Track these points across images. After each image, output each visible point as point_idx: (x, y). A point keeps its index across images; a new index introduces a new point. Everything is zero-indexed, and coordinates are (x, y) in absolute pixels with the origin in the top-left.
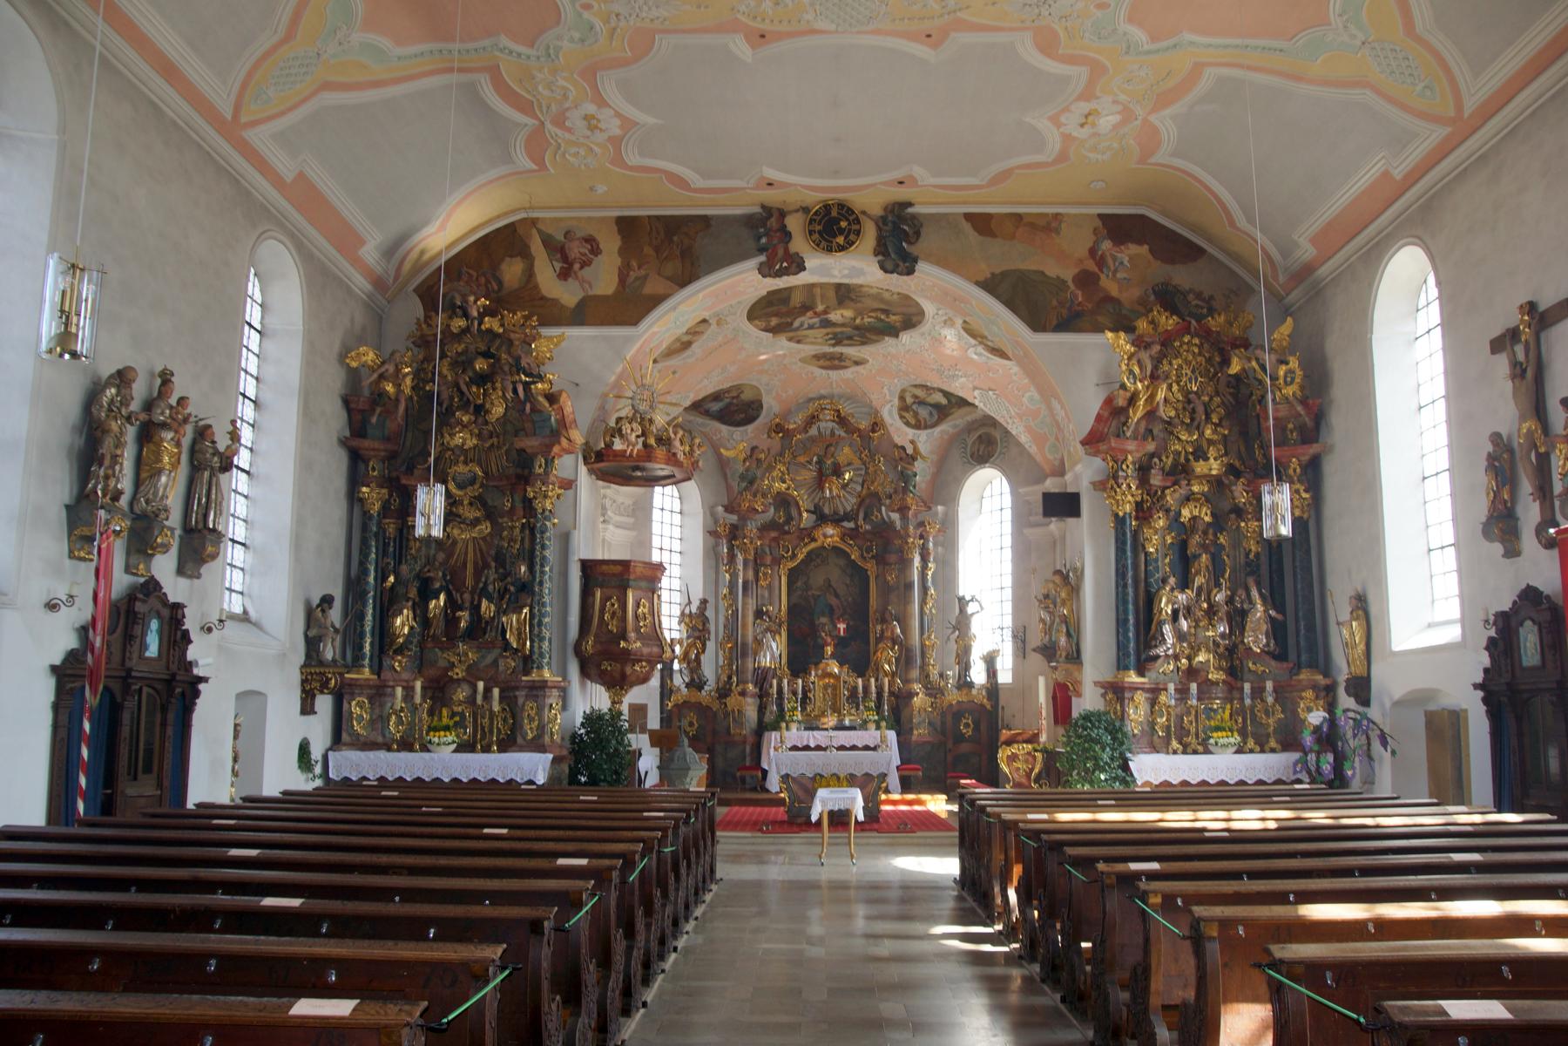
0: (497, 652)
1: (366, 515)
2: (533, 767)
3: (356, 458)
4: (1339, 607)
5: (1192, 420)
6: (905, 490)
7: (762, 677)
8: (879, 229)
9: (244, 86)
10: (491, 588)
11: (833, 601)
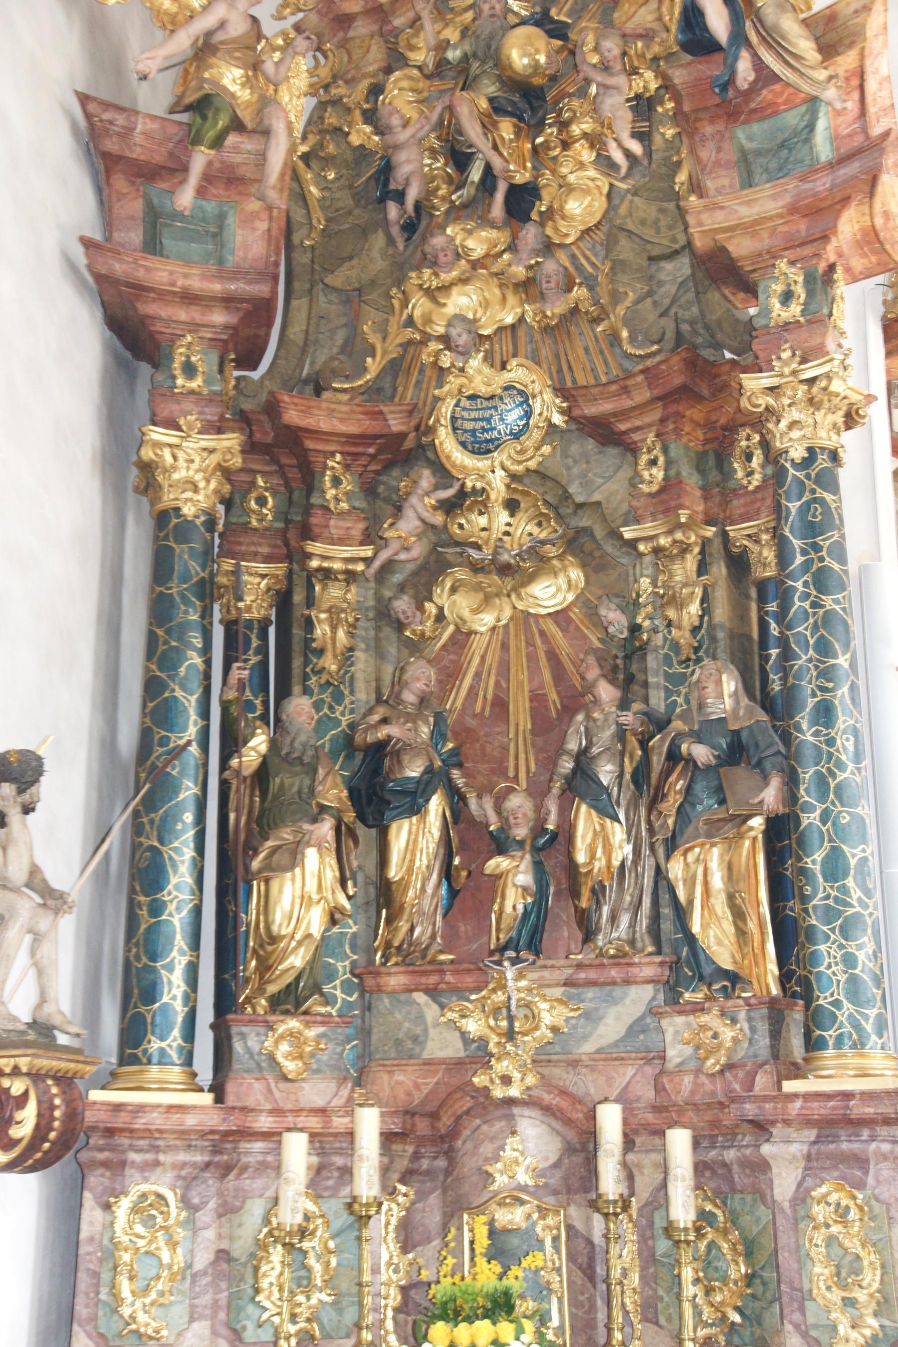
0: (639, 998)
3: (133, 337)
10: (606, 773)
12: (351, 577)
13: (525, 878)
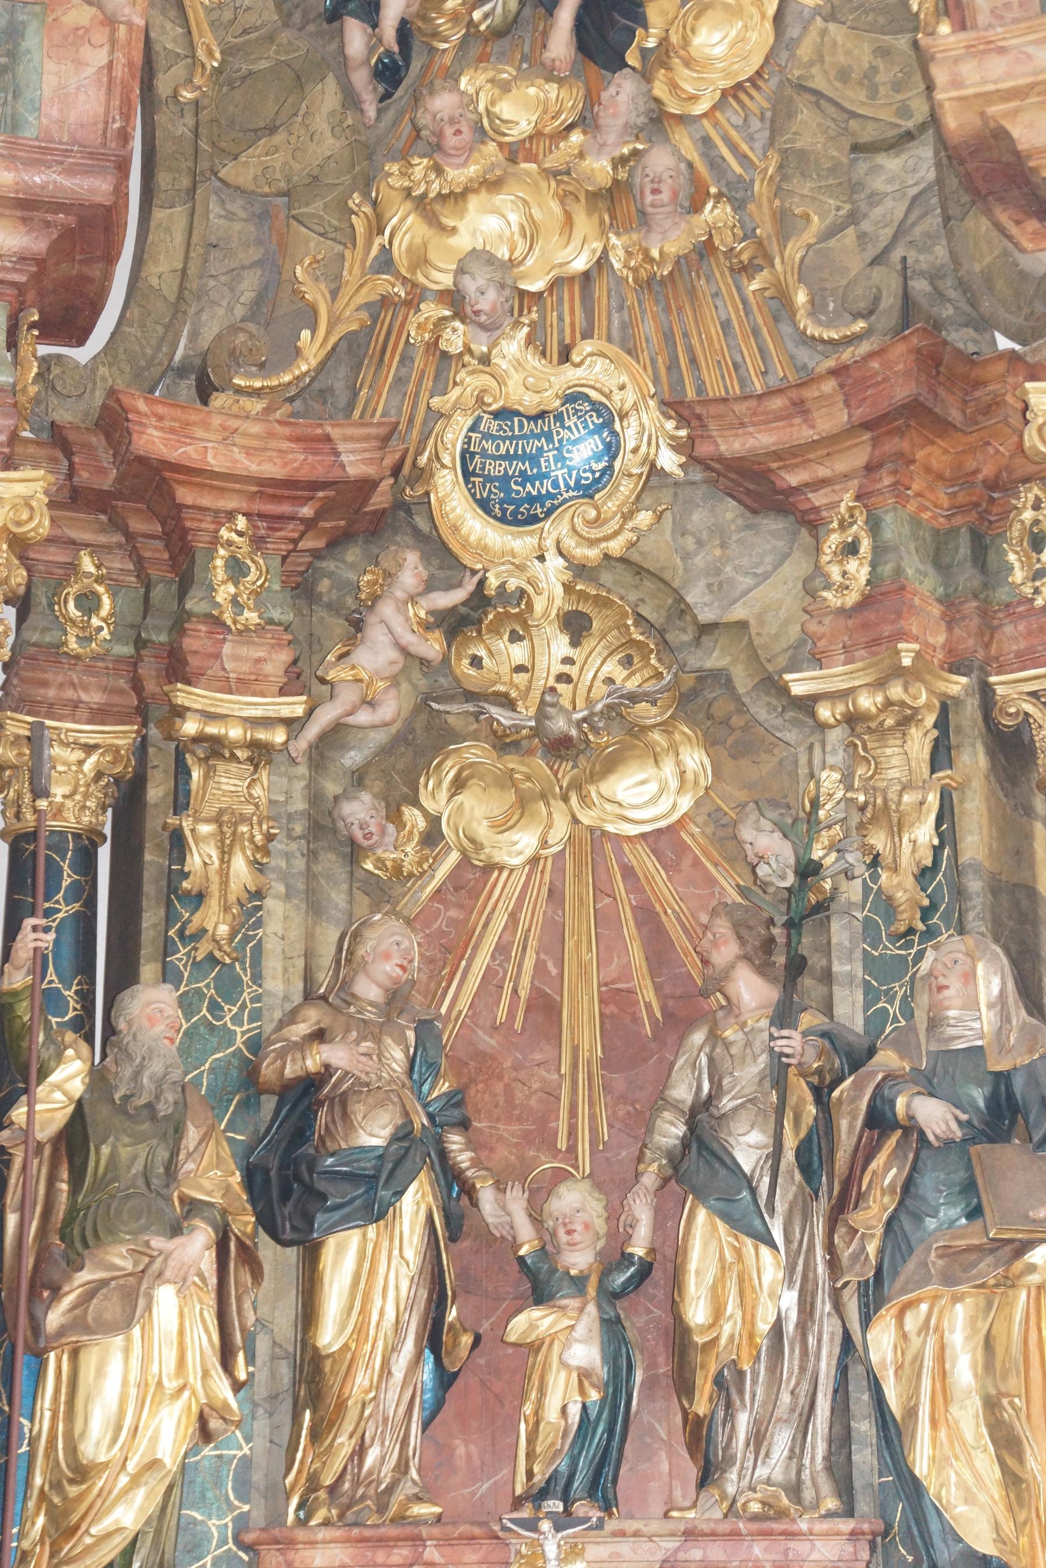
10: (748, 1147)
12: (260, 754)
13: (585, 1351)
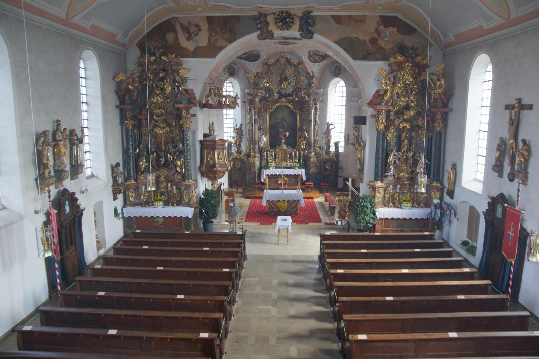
1: (127, 130)
2: (188, 212)
4: (448, 167)
5: (406, 94)
6: (310, 88)
7: (261, 151)
8: (301, 21)
9: (69, 7)
11: (285, 124)
